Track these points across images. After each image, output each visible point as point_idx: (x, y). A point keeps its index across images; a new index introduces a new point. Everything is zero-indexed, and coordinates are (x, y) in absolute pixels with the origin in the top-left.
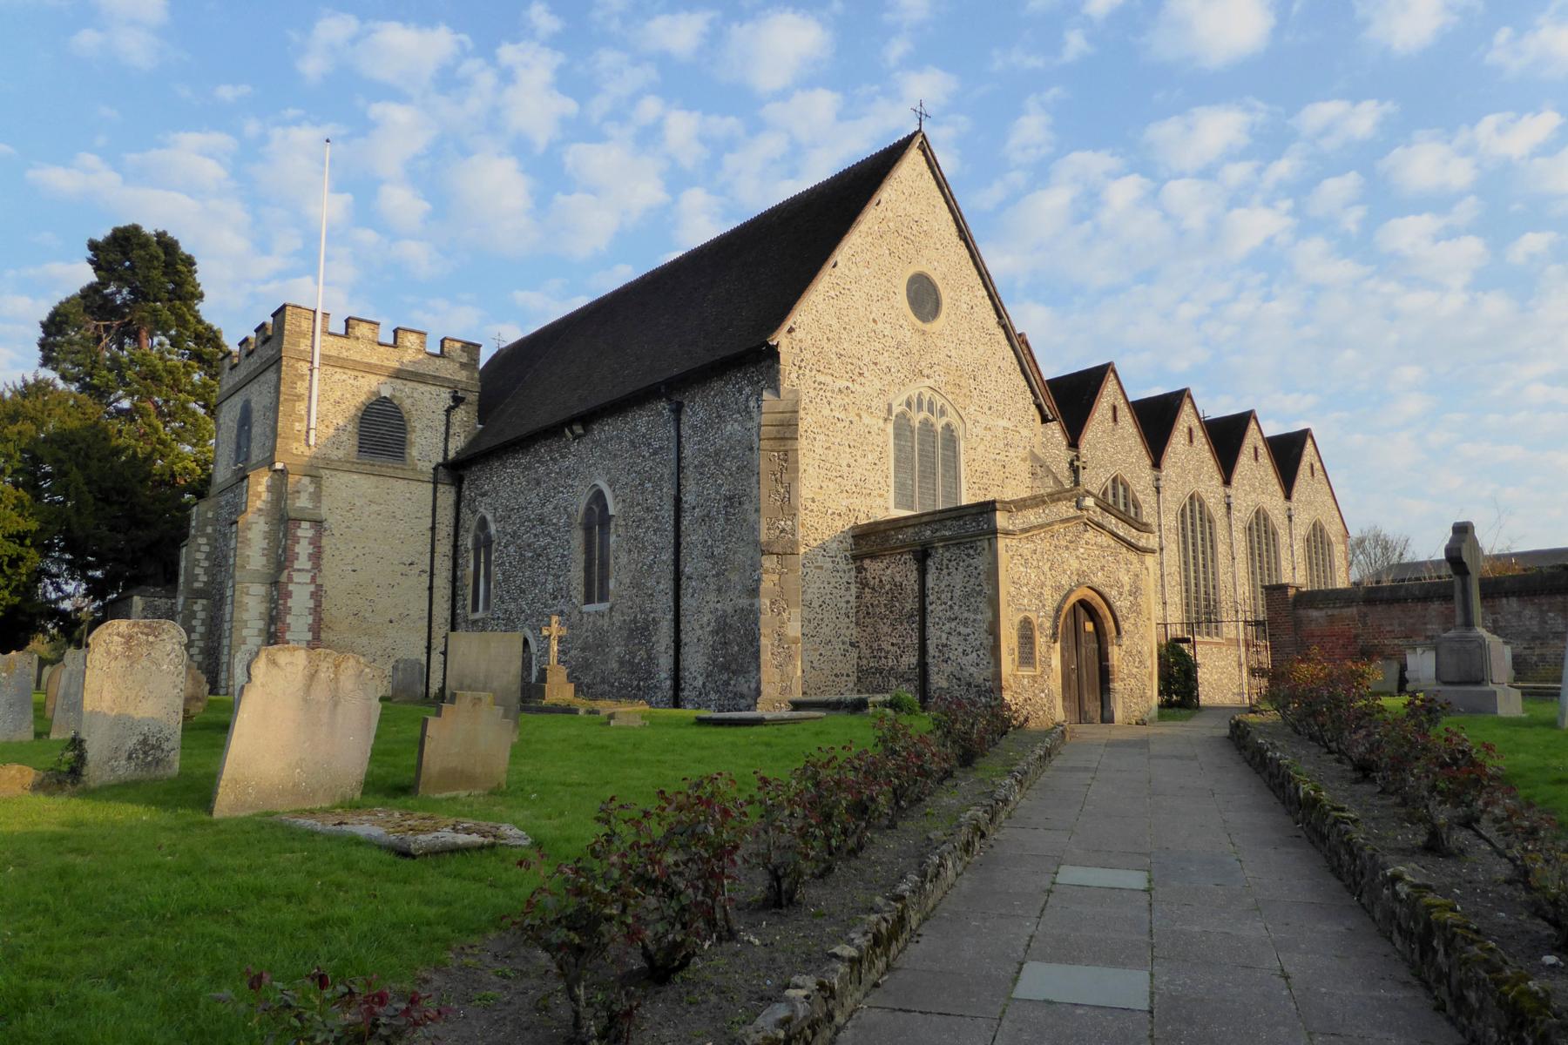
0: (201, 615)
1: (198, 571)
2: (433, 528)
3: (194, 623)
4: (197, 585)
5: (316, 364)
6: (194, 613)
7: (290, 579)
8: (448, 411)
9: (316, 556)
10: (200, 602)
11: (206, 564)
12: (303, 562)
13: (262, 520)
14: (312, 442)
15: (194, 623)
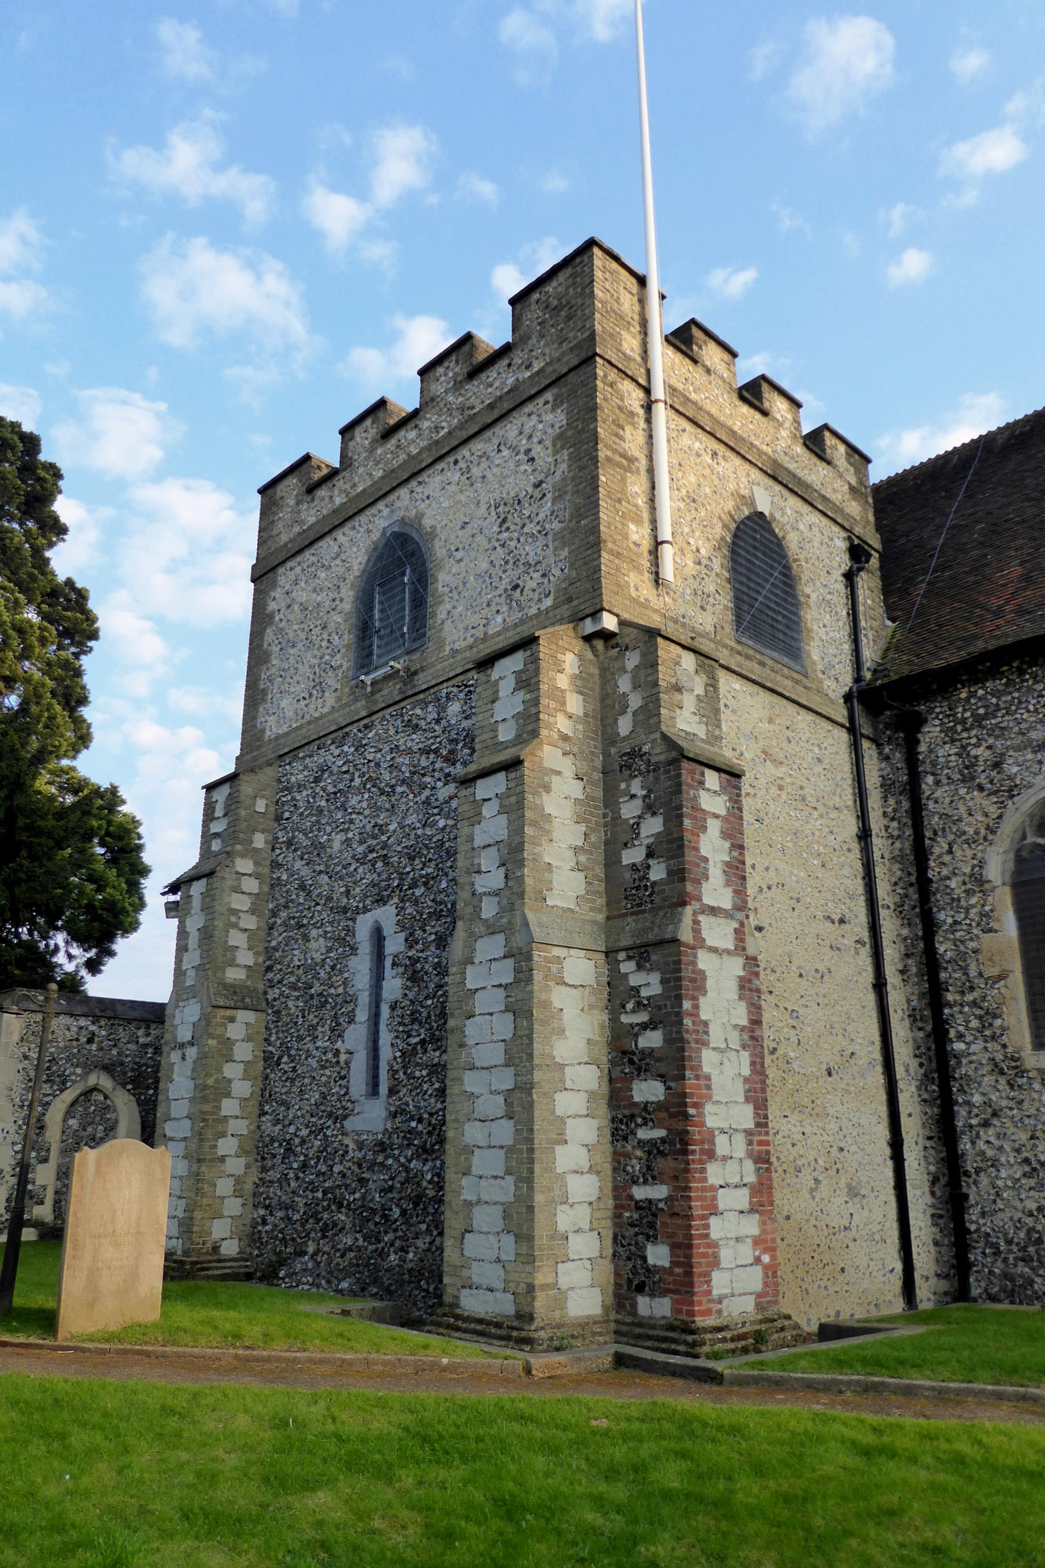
0: (244, 1051)
1: (236, 939)
2: (864, 835)
3: (231, 1071)
4: (234, 975)
5: (659, 392)
6: (228, 1043)
7: (697, 931)
8: (849, 577)
9: (736, 872)
10: (245, 1016)
11: (250, 922)
12: (715, 891)
13: (567, 766)
14: (668, 572)
15: (231, 1071)
